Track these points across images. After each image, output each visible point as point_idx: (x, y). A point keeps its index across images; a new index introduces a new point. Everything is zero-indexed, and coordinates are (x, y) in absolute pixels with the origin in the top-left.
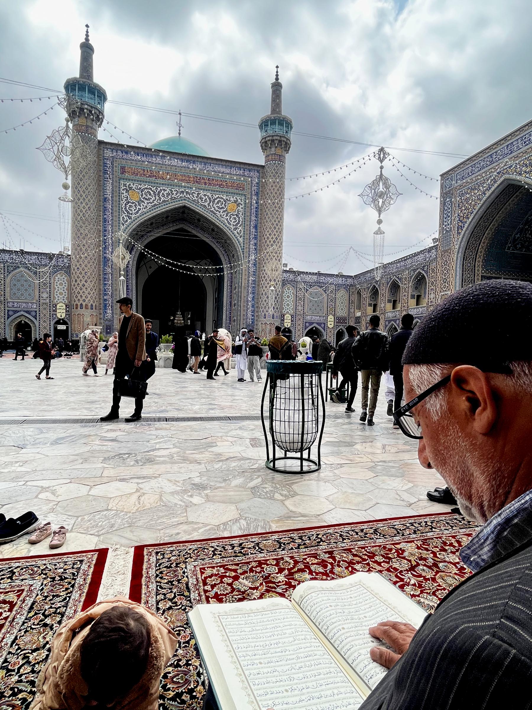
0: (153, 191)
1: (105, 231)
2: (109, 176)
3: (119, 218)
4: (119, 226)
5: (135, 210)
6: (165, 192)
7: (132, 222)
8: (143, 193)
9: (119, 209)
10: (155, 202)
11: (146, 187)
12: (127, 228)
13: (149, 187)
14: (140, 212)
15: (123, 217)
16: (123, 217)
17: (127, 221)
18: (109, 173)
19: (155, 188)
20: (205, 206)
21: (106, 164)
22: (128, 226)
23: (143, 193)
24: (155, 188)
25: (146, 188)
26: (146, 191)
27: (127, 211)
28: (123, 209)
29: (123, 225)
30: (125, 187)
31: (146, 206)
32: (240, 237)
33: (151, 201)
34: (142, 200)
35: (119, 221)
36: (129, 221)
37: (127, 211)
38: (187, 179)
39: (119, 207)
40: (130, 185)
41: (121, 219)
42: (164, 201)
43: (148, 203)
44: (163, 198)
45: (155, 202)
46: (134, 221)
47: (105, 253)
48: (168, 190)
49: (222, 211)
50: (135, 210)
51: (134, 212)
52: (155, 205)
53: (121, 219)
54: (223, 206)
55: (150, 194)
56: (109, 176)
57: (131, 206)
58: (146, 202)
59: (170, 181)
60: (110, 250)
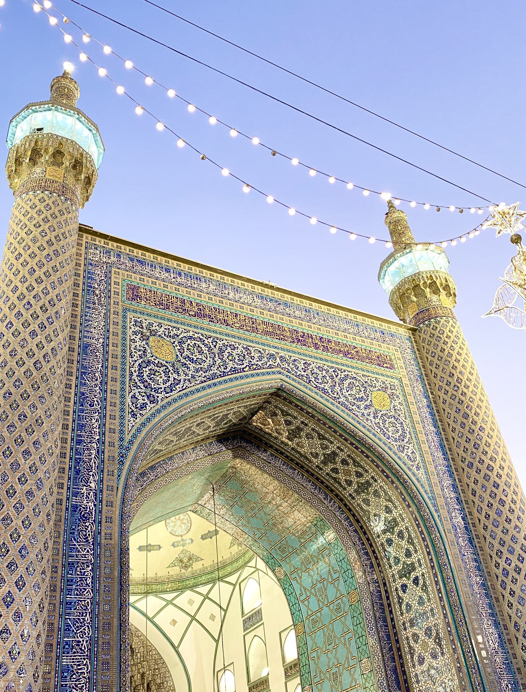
0: (206, 345)
1: (81, 427)
2: (99, 299)
3: (123, 397)
4: (122, 417)
5: (165, 382)
6: (235, 352)
7: (159, 411)
8: (185, 346)
9: (123, 376)
10: (214, 370)
11: (191, 334)
12: (143, 425)
13: (196, 336)
14: (179, 387)
15: (134, 397)
16: (134, 397)
17: (143, 406)
18: (97, 292)
19: (210, 340)
20: (324, 391)
21: (93, 273)
22: (149, 420)
23: (185, 346)
24: (210, 340)
25: (190, 338)
26: (191, 342)
27: (143, 382)
28: (134, 377)
29: (134, 415)
30: (137, 328)
31: (193, 377)
32: (418, 468)
33: (205, 365)
34: (183, 361)
35: (123, 403)
36: (149, 406)
37: (143, 382)
38: (278, 332)
39: (124, 370)
40: (151, 324)
41: (128, 400)
42: (235, 371)
43: (197, 371)
44: (230, 365)
45: (214, 370)
46: (164, 407)
47: (76, 494)
48: (240, 347)
49: (362, 405)
50: (165, 382)
51: (163, 386)
52: (214, 377)
53: (128, 400)
54: (362, 394)
55: (201, 352)
56: (99, 299)
57: (153, 372)
58: (192, 366)
59: (241, 331)
60: (93, 485)
